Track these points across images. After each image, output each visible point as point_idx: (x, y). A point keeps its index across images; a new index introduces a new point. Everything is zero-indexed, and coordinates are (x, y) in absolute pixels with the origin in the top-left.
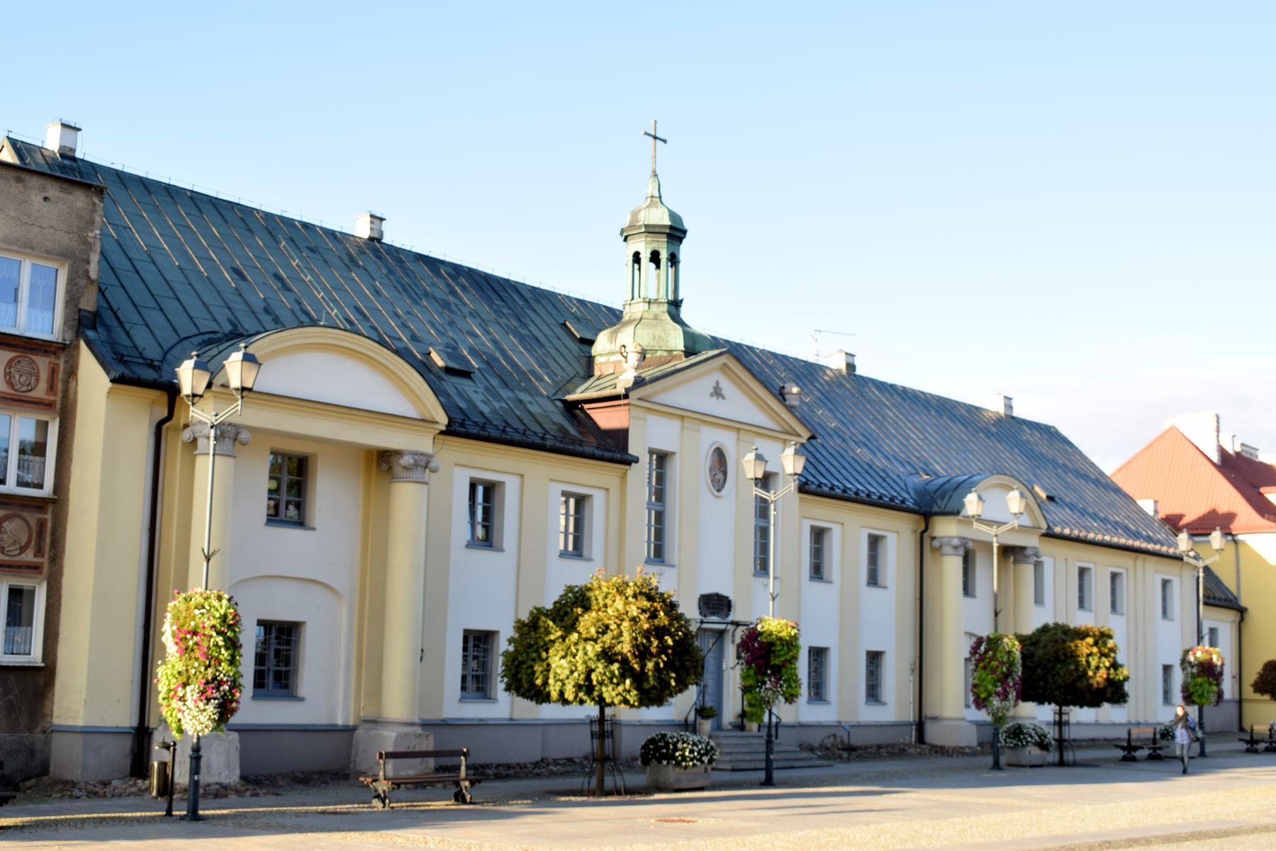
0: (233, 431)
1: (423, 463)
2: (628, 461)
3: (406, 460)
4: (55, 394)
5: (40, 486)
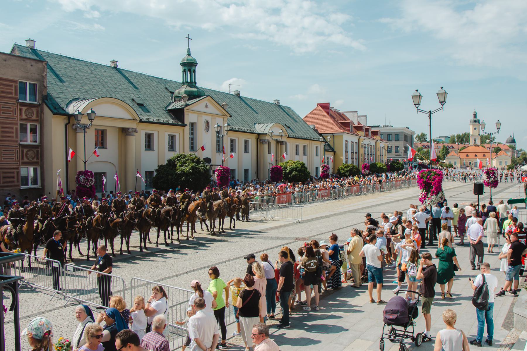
1: (134, 131)
2: (184, 125)
3: (130, 130)
4: (38, 118)
5: (36, 142)
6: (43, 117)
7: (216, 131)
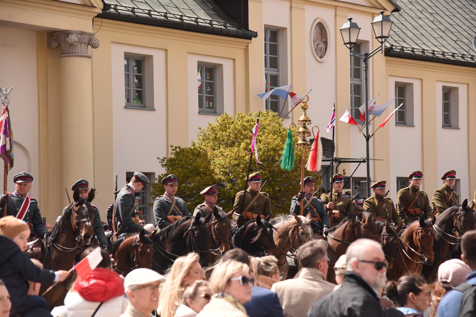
1: (86, 41)
2: (251, 36)
3: (73, 38)
7: (347, 40)
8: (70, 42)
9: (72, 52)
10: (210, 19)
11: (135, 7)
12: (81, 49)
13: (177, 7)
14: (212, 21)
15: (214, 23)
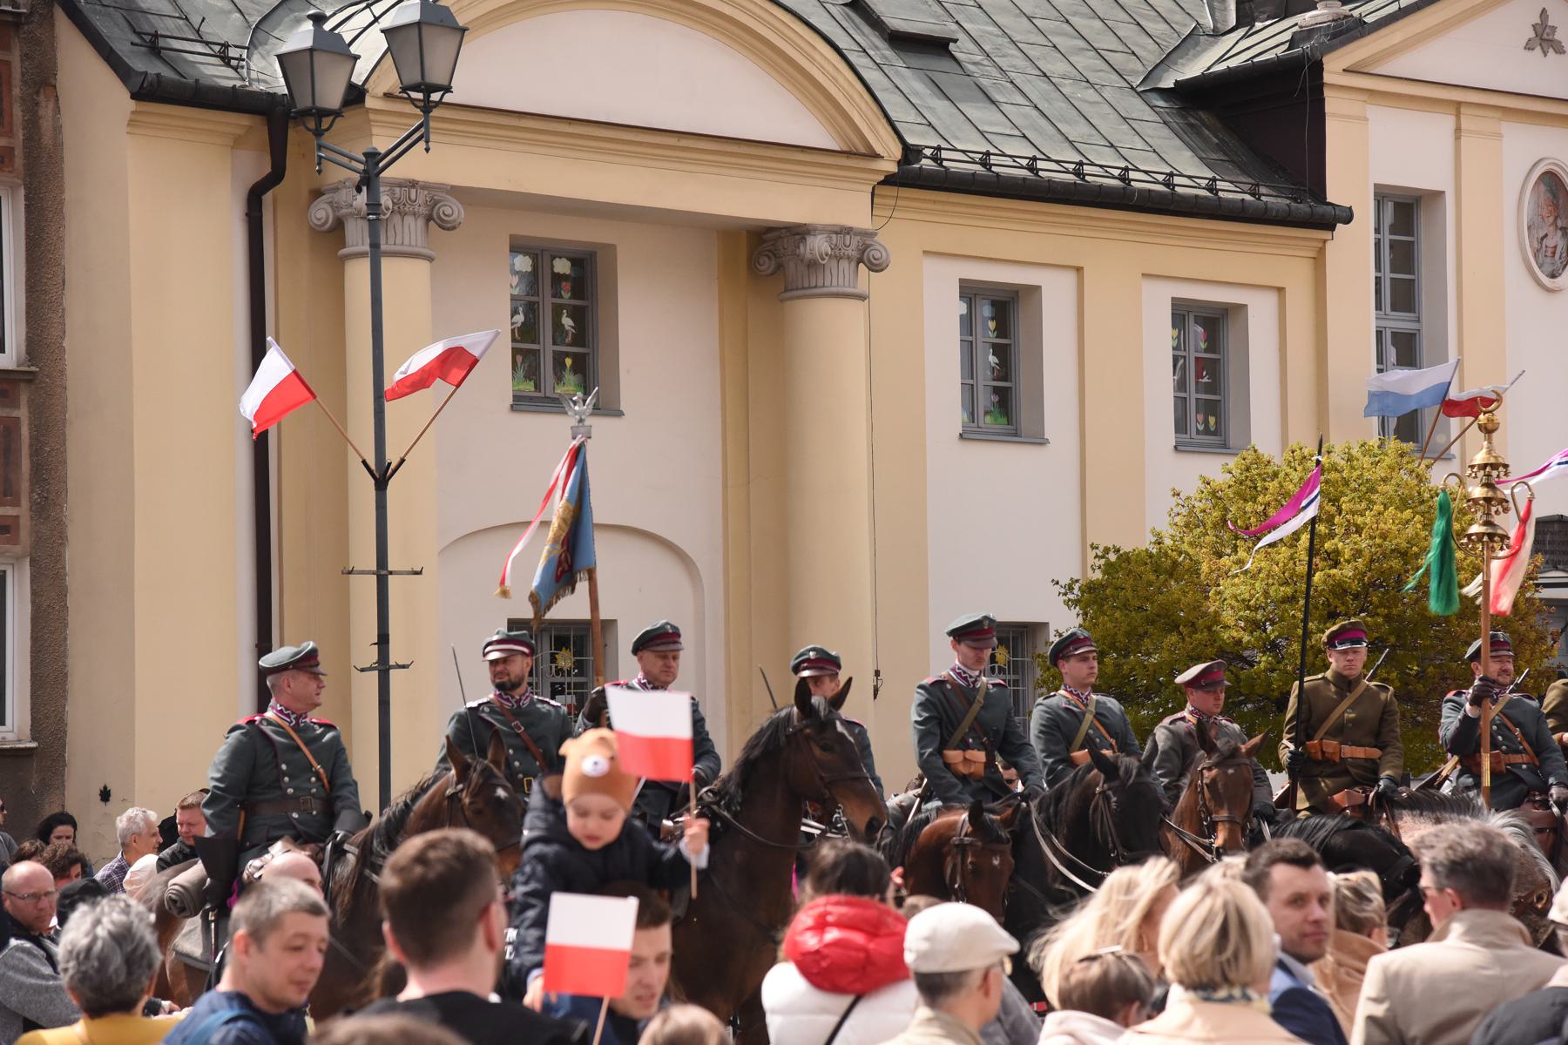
0: (420, 201)
1: (852, 252)
2: (1330, 219)
3: (818, 245)
6: (58, 129)
8: (808, 256)
9: (813, 284)
10: (1210, 174)
11: (993, 150)
12: (839, 275)
13: (1112, 146)
14: (1214, 180)
15: (1220, 185)
